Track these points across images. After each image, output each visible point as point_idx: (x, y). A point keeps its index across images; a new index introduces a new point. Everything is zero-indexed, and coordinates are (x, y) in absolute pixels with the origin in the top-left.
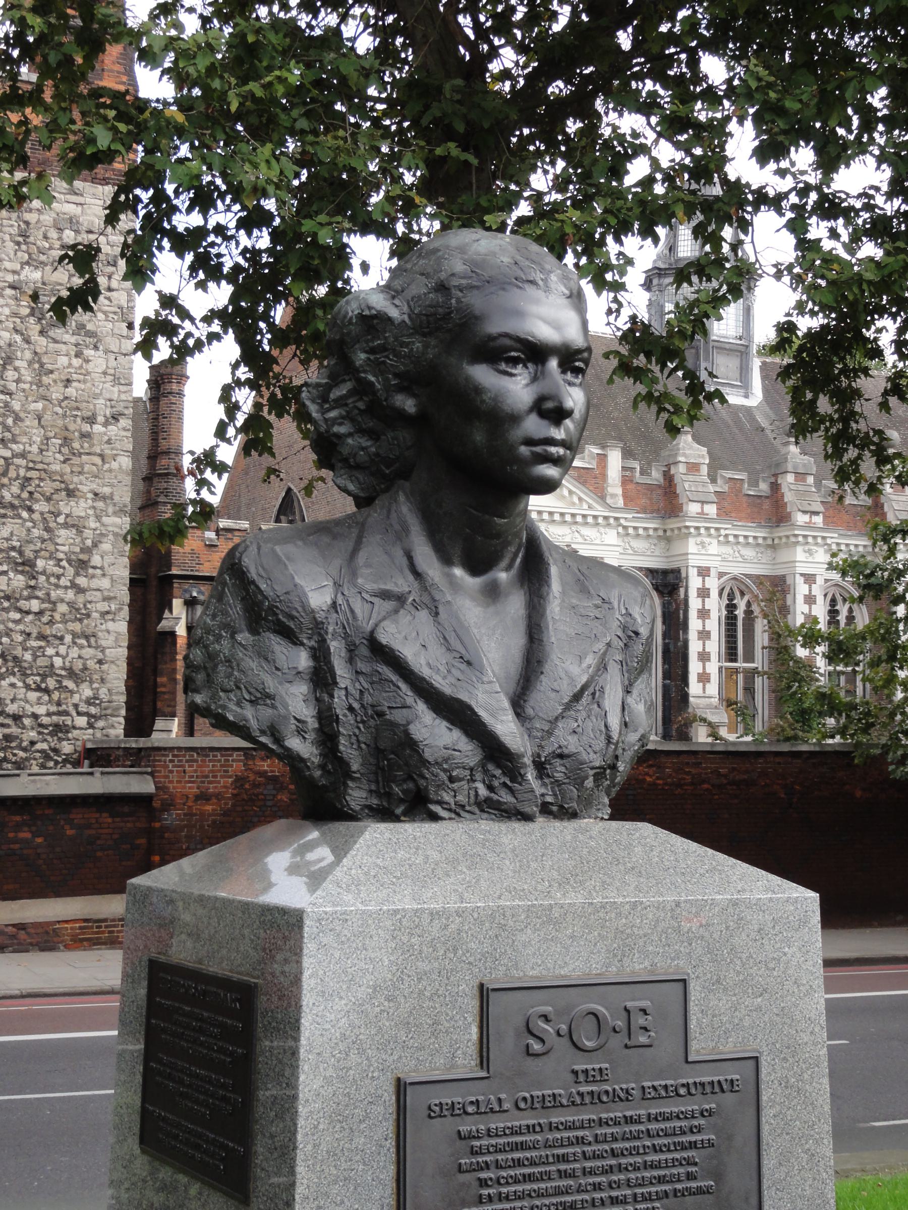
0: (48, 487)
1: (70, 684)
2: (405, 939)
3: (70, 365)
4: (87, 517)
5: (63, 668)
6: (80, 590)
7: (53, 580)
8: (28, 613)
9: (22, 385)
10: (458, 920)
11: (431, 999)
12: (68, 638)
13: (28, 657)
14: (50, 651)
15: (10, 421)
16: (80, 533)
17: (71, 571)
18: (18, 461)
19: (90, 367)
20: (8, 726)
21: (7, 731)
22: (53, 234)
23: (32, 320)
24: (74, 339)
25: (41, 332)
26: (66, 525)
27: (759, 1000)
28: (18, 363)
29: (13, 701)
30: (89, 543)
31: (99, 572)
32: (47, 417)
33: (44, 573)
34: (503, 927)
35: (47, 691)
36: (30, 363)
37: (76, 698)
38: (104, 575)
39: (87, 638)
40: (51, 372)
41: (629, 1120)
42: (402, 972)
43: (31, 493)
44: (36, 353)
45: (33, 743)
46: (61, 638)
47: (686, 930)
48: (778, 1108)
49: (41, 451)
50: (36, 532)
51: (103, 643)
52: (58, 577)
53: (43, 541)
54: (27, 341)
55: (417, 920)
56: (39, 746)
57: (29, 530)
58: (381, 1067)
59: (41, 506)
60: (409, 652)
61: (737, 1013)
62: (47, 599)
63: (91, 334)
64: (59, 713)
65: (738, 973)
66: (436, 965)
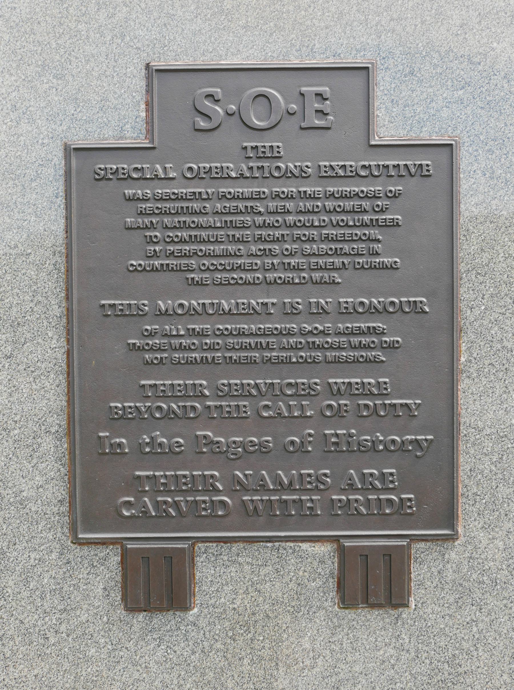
2: (73, 25)
10: (125, 9)
11: (99, 78)
27: (461, 92)
34: (171, 16)
42: (70, 54)
47: (374, 23)
48: (481, 197)
55: (84, 9)
58: (51, 135)
61: (434, 104)
65: (436, 66)
66: (103, 49)
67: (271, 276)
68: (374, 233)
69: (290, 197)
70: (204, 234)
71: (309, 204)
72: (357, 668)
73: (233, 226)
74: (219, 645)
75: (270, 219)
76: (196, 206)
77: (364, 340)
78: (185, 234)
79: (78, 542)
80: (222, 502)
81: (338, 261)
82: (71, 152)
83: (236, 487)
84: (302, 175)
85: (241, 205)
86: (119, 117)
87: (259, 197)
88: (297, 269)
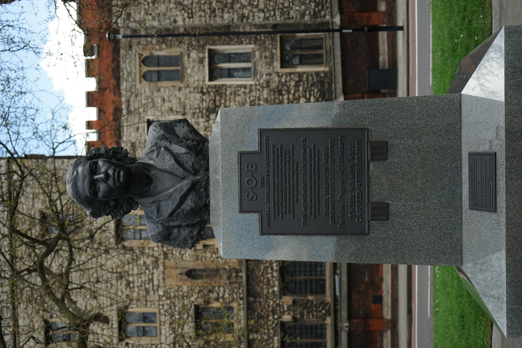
34: (227, 206)
41: (274, 171)
60: (169, 211)
67: (295, 180)
68: (283, 152)
69: (274, 175)
70: (284, 198)
72: (406, 156)
73: (282, 190)
74: (399, 195)
75: (280, 180)
76: (276, 200)
77: (313, 154)
78: (284, 203)
79: (369, 234)
80: (358, 194)
81: (291, 162)
82: (262, 233)
83: (353, 189)
84: (268, 171)
85: (276, 188)
87: (274, 183)
88: (293, 173)
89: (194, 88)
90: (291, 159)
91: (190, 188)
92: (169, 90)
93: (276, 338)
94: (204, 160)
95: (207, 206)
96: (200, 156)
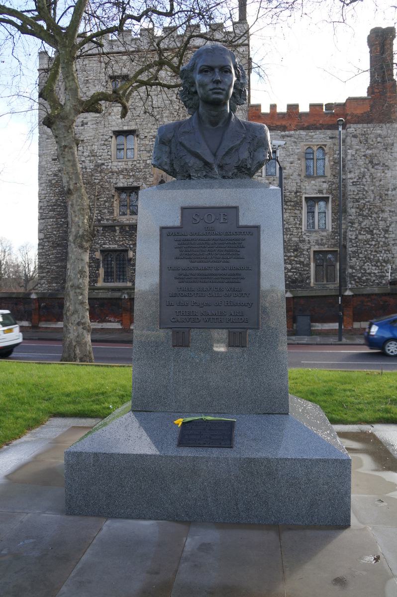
0: (376, 210)
1: (384, 264)
3: (381, 176)
4: (387, 218)
5: (382, 260)
6: (386, 238)
7: (378, 236)
8: (372, 245)
9: (368, 183)
12: (383, 252)
13: (372, 257)
14: (378, 255)
15: (365, 193)
16: (386, 222)
17: (383, 233)
18: (367, 204)
19: (387, 175)
20: (367, 276)
21: (367, 277)
22: (374, 140)
23: (370, 164)
24: (382, 168)
25: (373, 167)
26: (381, 220)
28: (366, 177)
29: (368, 269)
30: (388, 225)
31: (391, 233)
32: (375, 190)
33: (376, 234)
35: (378, 266)
36: (370, 176)
37: (386, 268)
38: (393, 233)
39: (389, 251)
40: (376, 178)
43: (371, 212)
44: (371, 173)
45: (374, 281)
46: (381, 252)
49: (374, 200)
50: (373, 223)
51: (394, 252)
52: (380, 235)
53: (375, 225)
54: (368, 170)
56: (376, 281)
57: (371, 222)
59: (374, 216)
60: (186, 143)
62: (377, 241)
63: (386, 166)
64: (381, 272)
71: (221, 242)
75: (211, 246)
77: (236, 277)
82: (162, 228)
86: (175, 220)
89: (300, 186)
90: (231, 256)
91: (206, 161)
92: (299, 167)
93: (116, 246)
94: (232, 174)
95: (189, 177)
96: (236, 171)
